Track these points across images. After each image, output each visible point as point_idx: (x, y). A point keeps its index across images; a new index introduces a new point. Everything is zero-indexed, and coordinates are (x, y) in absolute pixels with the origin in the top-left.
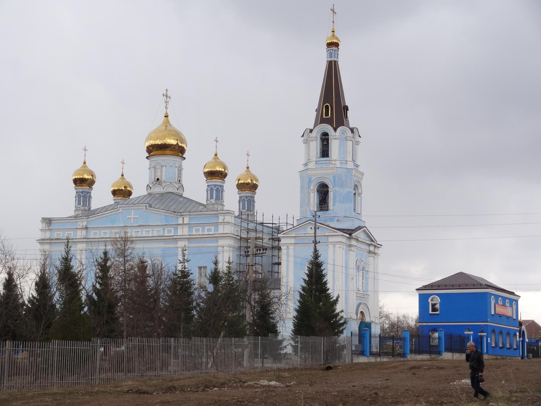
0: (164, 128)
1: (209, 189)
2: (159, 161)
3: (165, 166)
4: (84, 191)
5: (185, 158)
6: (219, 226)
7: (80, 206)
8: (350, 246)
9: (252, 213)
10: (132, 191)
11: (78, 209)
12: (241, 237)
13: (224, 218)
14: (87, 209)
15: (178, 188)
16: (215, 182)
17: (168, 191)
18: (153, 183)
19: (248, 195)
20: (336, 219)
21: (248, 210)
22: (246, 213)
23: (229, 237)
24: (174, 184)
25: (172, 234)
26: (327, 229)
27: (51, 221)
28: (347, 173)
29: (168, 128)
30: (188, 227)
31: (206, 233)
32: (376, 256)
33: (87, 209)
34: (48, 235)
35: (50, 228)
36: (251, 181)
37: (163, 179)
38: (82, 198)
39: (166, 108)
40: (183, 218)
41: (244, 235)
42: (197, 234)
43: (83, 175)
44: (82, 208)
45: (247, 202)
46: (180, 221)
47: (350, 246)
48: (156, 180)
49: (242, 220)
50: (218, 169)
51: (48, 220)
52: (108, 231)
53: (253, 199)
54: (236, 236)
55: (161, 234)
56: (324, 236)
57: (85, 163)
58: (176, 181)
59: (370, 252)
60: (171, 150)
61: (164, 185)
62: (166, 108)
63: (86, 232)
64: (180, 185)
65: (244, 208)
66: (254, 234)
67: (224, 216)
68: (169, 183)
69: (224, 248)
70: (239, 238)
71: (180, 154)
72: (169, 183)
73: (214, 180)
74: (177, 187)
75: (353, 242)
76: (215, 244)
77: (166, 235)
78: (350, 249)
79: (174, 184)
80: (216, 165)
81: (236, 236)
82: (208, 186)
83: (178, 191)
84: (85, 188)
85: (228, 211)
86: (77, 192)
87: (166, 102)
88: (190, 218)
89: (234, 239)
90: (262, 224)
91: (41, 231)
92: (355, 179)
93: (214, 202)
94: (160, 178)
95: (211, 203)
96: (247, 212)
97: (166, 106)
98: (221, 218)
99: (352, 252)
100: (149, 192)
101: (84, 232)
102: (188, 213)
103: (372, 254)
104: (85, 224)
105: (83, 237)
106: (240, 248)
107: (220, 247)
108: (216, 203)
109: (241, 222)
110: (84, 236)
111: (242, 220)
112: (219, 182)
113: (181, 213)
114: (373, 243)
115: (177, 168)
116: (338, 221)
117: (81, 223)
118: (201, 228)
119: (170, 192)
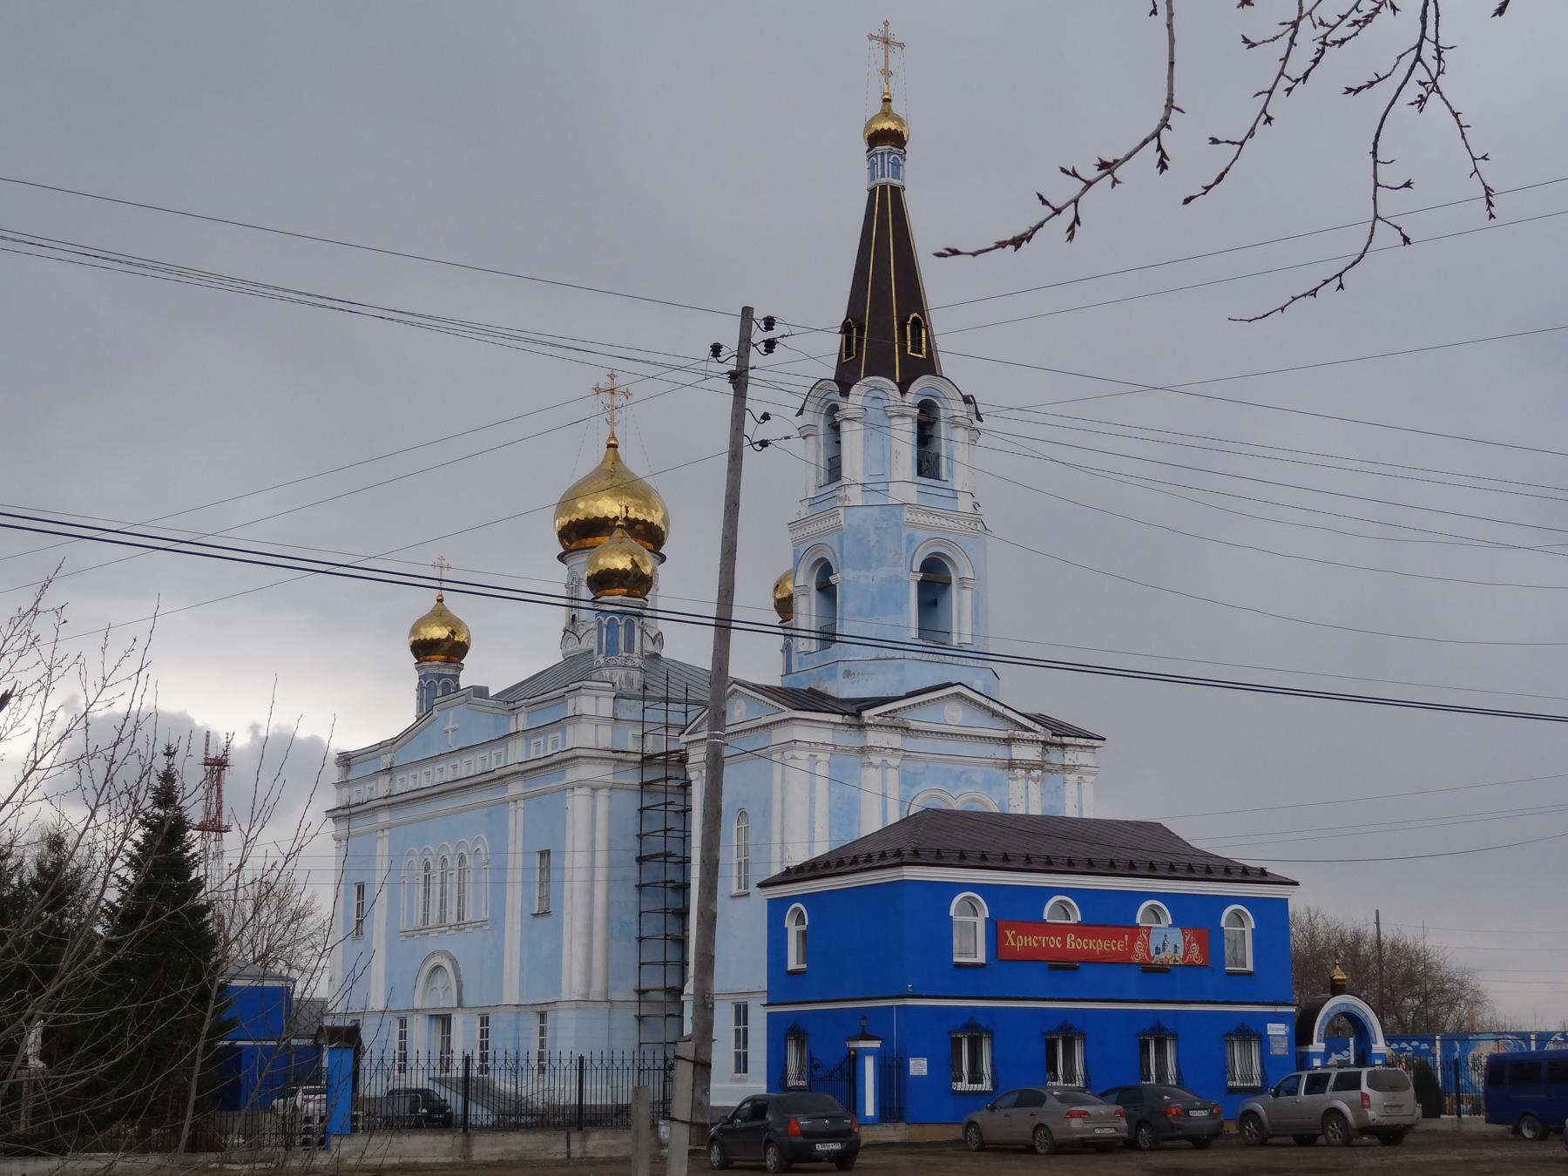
4: (430, 672)
8: (863, 750)
12: (642, 754)
20: (842, 667)
26: (917, 706)
27: (349, 759)
28: (884, 520)
32: (1072, 778)
38: (425, 690)
47: (863, 750)
49: (647, 704)
56: (757, 727)
59: (1011, 765)
69: (576, 793)
70: (639, 758)
75: (874, 738)
78: (865, 760)
92: (922, 535)
99: (872, 771)
103: (1028, 770)
108: (607, 665)
109: (643, 711)
114: (1027, 735)
116: (848, 674)
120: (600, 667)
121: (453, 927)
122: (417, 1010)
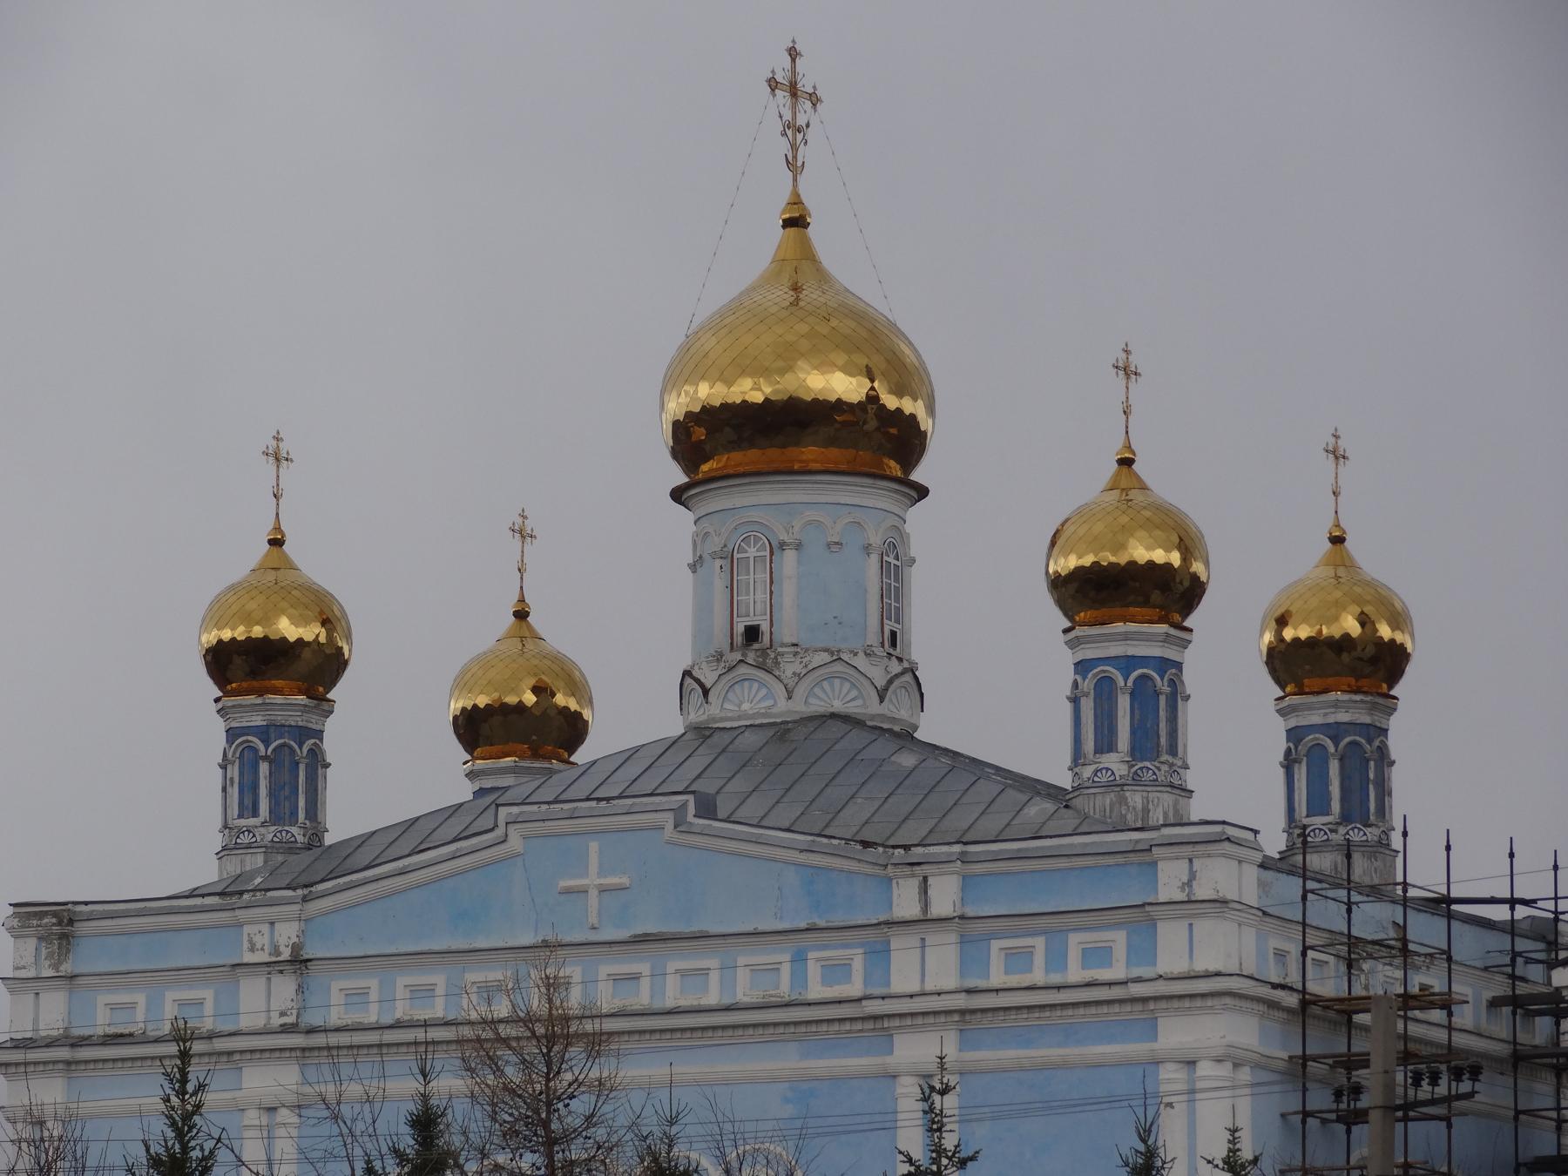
0: (783, 295)
1: (1088, 685)
2: (755, 515)
3: (798, 546)
5: (922, 492)
6: (1160, 925)
7: (252, 821)
9: (1372, 834)
10: (587, 714)
11: (245, 839)
13: (1192, 876)
14: (300, 838)
15: (886, 689)
16: (1126, 637)
17: (818, 706)
18: (719, 656)
19: (1343, 717)
21: (1346, 818)
22: (1333, 836)
23: (1228, 1000)
24: (860, 662)
25: (855, 988)
27: (71, 922)
29: (811, 295)
30: (953, 938)
31: (1075, 974)
33: (300, 838)
34: (53, 1013)
35: (67, 968)
36: (1363, 625)
37: (786, 633)
38: (264, 768)
39: (794, 166)
40: (925, 879)
41: (1327, 982)
42: (1014, 980)
43: (266, 620)
44: (269, 834)
45: (1342, 768)
46: (905, 903)
48: (739, 640)
49: (1311, 885)
50: (1142, 552)
51: (55, 914)
52: (439, 980)
53: (1377, 743)
54: (1275, 986)
55: (785, 989)
57: (277, 543)
58: (873, 638)
60: (831, 442)
61: (790, 668)
62: (794, 166)
63: (300, 989)
64: (896, 668)
65: (1318, 804)
66: (1389, 971)
67: (1191, 861)
68: (826, 657)
70: (1292, 1000)
71: (892, 463)
72: (826, 657)
73: (1119, 627)
74: (880, 683)
76: (1136, 1049)
77: (816, 991)
79: (860, 662)
80: (1128, 531)
81: (1275, 986)
82: (1082, 667)
83: (886, 708)
84: (287, 706)
85: (1218, 828)
86: (232, 734)
87: (789, 133)
88: (966, 879)
89: (1262, 1008)
90: (1442, 905)
91: (12, 991)
93: (1121, 770)
94: (765, 627)
95: (1104, 778)
96: (1342, 830)
97: (795, 157)
98: (1169, 879)
100: (696, 716)
101: (284, 988)
102: (957, 848)
104: (287, 934)
105: (277, 1021)
106: (1304, 1066)
107: (1171, 1066)
108: (1136, 780)
109: (1304, 898)
110: (283, 1014)
111: (1311, 885)
112: (1149, 638)
113: (906, 848)
115: (874, 558)
117: (266, 928)
118: (1039, 943)
119: (833, 716)
120: (1111, 785)
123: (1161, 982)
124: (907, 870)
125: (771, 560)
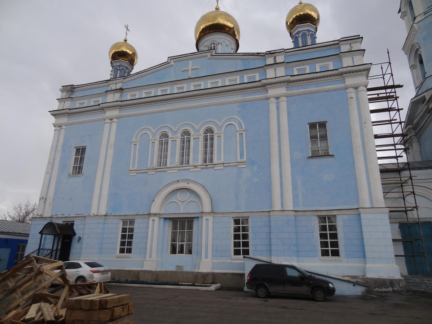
2: (214, 39)
4: (123, 65)
27: (74, 88)
30: (284, 68)
34: (68, 105)
38: (119, 71)
40: (275, 57)
63: (121, 96)
91: (59, 102)
117: (115, 85)
121: (199, 167)
122: (155, 215)
123: (349, 68)
124: (271, 55)
125: (216, 46)
